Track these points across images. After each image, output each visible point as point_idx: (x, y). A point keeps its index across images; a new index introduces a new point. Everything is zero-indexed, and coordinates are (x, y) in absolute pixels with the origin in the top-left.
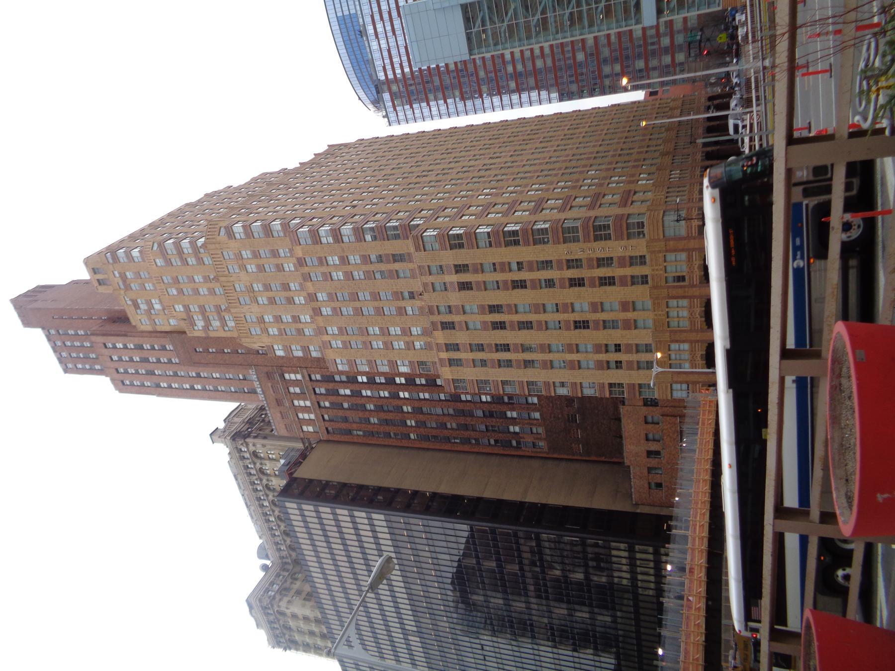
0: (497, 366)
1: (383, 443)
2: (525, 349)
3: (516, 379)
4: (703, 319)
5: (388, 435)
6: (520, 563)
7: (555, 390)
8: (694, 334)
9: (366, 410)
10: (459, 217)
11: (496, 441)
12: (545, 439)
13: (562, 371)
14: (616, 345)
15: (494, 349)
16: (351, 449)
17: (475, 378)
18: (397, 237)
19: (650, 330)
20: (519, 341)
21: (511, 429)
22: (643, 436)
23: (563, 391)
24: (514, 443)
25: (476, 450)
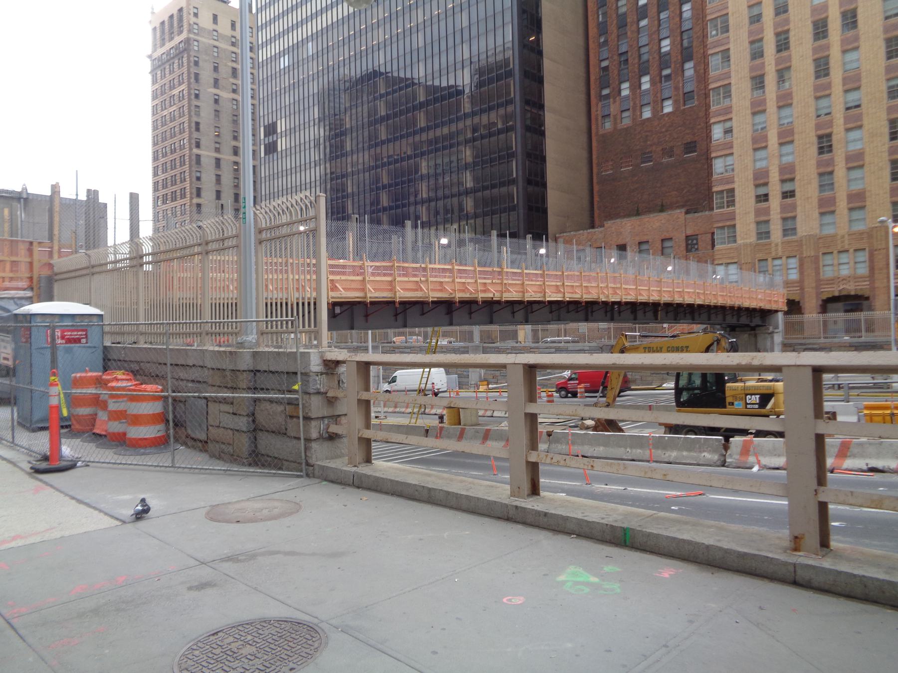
0: (751, 39)
2: (782, 74)
3: (733, 67)
6: (473, 114)
7: (719, 122)
8: (814, 285)
11: (606, 69)
12: (615, 128)
13: (749, 128)
14: (793, 191)
15: (780, 30)
17: (730, 10)
19: (818, 231)
20: (795, 62)
21: (625, 85)
22: (645, 238)
23: (717, 132)
24: (605, 92)
25: (591, 45)
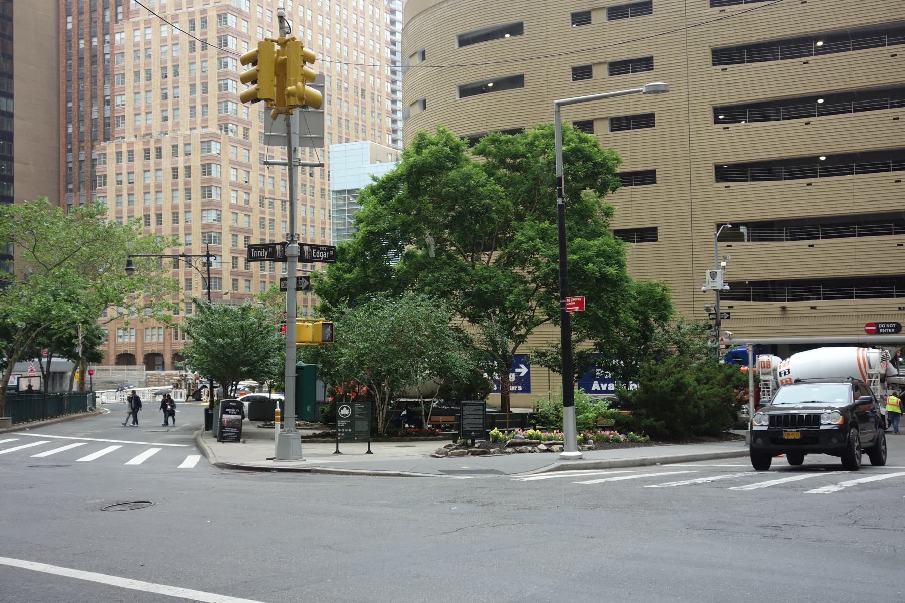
1: (61, 51)
4: (150, 352)
5: (69, 58)
9: (92, 37)
10: (233, 166)
11: (71, 169)
16: (52, 14)
18: (220, 110)
24: (70, 187)
25: (62, 150)
